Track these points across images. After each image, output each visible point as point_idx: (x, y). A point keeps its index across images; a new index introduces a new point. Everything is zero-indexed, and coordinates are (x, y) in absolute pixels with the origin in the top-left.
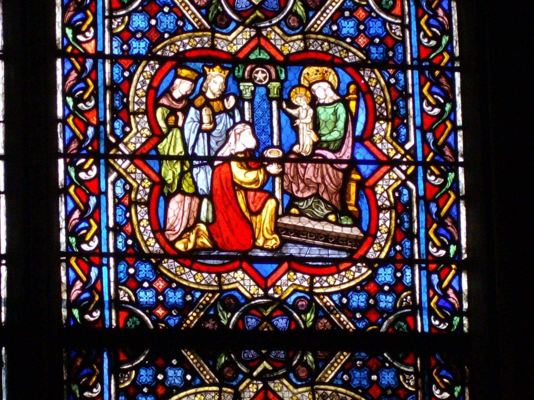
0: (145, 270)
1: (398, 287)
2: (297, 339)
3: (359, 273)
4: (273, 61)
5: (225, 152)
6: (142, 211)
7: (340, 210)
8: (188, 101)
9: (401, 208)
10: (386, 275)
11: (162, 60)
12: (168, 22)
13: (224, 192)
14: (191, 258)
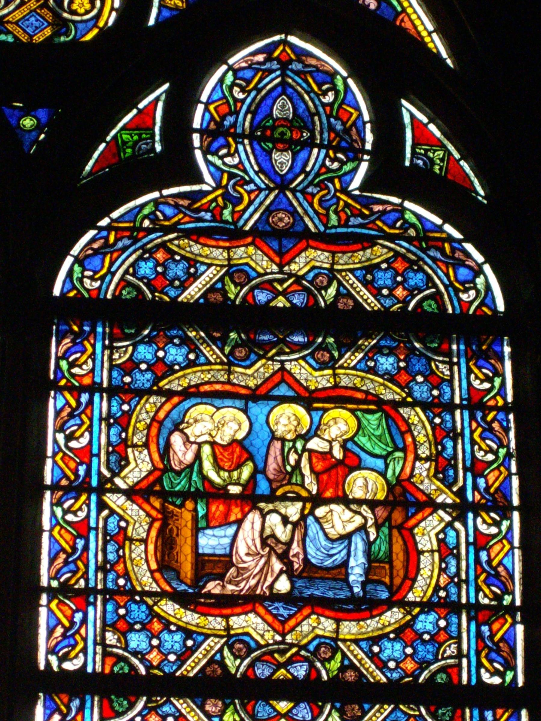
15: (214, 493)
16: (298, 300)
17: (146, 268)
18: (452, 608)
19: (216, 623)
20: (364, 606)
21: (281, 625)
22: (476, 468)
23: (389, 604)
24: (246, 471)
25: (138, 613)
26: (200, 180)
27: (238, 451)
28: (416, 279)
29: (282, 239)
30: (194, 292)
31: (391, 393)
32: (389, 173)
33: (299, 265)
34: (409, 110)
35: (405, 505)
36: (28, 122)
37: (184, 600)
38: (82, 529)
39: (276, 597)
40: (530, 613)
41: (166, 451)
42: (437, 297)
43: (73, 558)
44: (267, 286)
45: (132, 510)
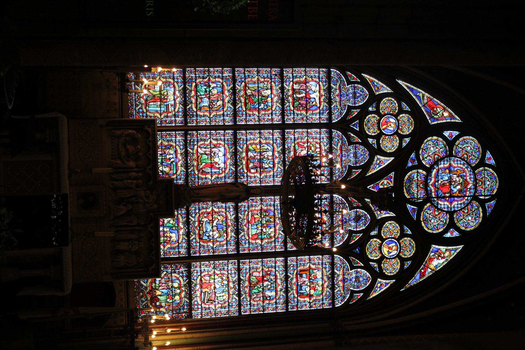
3: (200, 303)
6: (207, 273)
7: (208, 300)
8: (222, 279)
9: (209, 308)
12: (233, 275)
14: (201, 280)
15: (310, 275)
17: (338, 265)
18: (298, 302)
20: (297, 293)
22: (315, 304)
25: (295, 268)
27: (316, 277)
28: (339, 296)
29: (344, 280)
30: (336, 271)
31: (324, 294)
32: (353, 292)
33: (340, 283)
34: (362, 294)
38: (305, 261)
40: (297, 311)
41: (315, 269)
43: (301, 260)
44: (337, 279)
45: (308, 266)
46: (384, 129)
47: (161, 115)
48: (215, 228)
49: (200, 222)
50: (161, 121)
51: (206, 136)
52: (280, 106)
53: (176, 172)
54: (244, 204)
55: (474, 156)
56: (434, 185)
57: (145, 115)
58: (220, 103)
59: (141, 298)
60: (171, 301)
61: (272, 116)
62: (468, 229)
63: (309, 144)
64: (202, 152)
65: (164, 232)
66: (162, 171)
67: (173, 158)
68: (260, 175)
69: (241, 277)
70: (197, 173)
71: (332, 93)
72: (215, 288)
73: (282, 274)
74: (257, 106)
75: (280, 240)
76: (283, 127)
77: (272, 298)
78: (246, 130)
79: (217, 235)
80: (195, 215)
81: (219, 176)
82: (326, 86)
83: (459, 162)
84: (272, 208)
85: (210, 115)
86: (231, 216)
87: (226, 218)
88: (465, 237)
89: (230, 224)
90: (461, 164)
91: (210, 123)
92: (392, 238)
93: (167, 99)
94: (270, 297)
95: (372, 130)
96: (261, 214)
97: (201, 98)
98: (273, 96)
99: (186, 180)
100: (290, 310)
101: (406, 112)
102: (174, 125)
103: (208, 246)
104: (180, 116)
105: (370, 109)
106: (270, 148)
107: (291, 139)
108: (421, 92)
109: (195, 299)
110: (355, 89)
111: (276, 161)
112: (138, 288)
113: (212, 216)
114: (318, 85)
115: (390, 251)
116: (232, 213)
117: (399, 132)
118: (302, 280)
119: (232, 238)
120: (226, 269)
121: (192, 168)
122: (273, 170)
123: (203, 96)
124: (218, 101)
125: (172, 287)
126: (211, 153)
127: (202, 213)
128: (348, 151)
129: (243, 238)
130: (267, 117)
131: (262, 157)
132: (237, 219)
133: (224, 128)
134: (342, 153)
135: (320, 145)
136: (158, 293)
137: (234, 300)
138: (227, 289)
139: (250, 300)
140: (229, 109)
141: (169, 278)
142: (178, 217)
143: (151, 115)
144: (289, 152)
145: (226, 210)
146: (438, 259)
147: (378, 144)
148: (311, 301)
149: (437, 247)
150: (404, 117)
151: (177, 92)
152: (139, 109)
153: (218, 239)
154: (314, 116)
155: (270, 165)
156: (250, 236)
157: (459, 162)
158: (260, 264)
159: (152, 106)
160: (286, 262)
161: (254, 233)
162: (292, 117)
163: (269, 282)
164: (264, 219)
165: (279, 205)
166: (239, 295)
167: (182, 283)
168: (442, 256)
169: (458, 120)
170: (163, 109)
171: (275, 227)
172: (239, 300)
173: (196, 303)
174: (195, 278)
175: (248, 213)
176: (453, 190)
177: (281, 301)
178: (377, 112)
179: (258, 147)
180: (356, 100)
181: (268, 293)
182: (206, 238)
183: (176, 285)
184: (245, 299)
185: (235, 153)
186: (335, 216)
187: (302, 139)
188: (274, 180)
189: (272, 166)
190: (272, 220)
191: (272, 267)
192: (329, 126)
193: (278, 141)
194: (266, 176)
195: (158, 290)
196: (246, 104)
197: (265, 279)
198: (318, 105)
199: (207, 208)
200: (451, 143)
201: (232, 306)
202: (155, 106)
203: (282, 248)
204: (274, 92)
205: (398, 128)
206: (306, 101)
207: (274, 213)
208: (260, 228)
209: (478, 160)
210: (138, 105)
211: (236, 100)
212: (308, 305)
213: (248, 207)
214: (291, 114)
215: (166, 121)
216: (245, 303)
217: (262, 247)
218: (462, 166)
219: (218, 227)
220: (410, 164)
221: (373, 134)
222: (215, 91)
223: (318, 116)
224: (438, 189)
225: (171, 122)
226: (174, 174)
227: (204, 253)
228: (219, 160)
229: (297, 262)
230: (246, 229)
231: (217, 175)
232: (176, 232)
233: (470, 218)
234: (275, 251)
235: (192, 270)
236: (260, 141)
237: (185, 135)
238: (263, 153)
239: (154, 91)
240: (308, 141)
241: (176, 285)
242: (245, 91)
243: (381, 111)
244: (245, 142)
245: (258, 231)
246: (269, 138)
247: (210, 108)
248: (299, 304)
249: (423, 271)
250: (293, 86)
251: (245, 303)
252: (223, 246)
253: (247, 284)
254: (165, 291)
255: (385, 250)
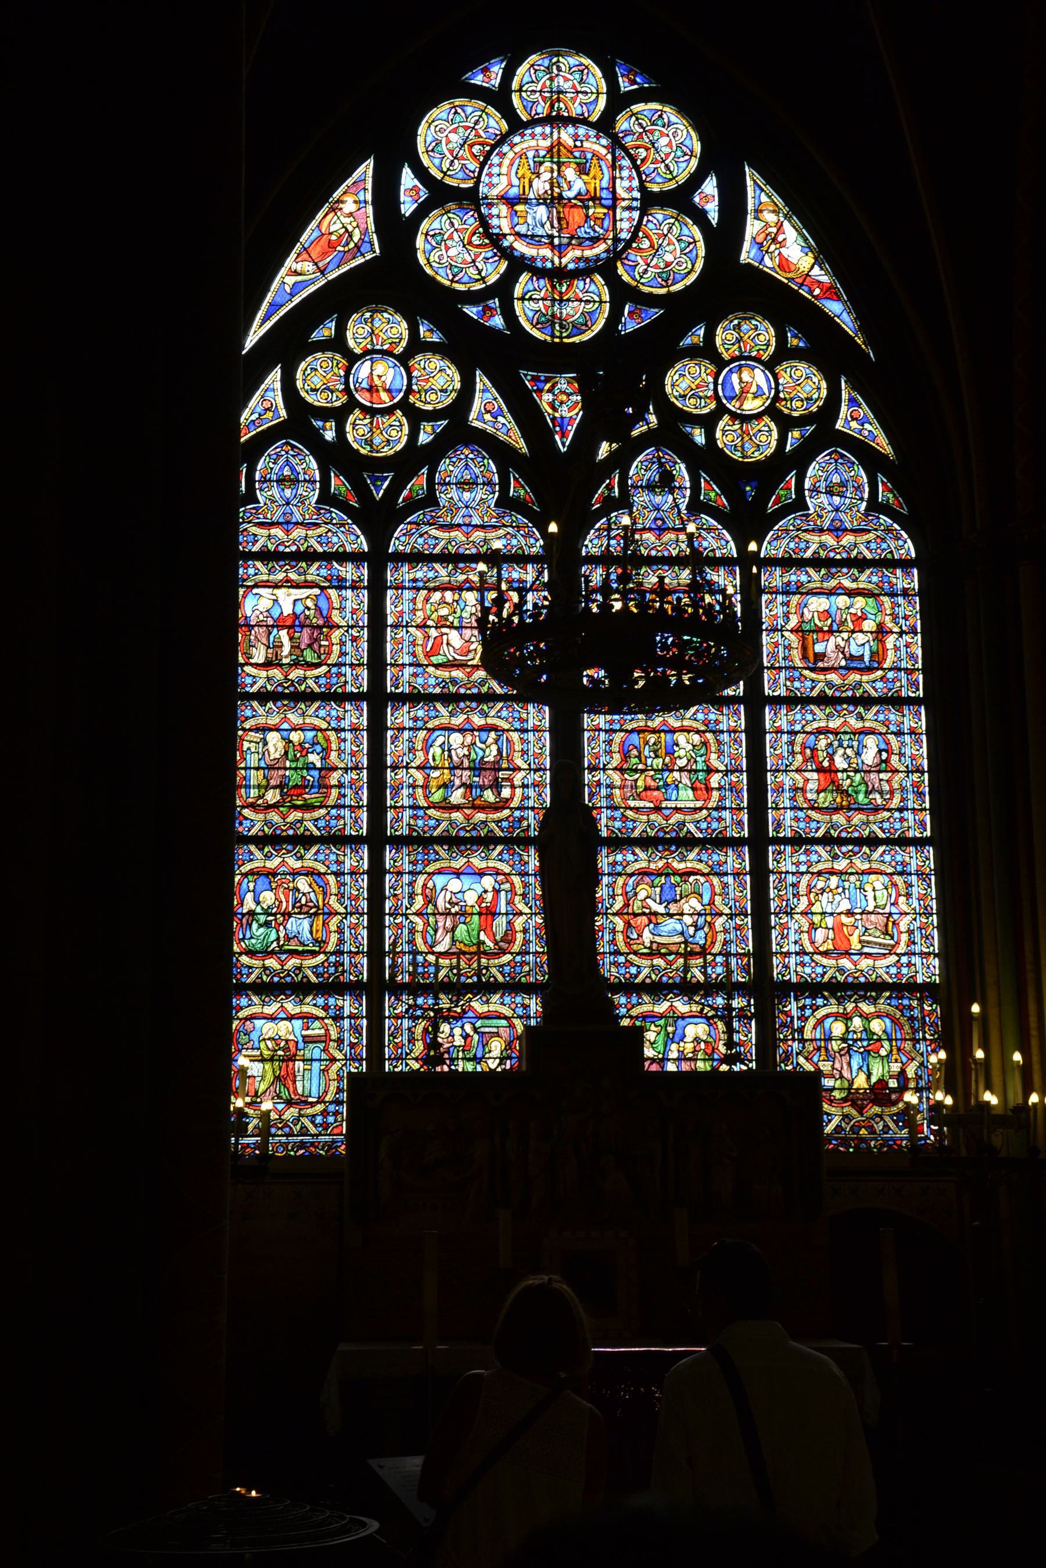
0: (807, 959)
1: (909, 965)
2: (869, 986)
3: (893, 959)
4: (857, 873)
5: (838, 911)
6: (806, 936)
7: (886, 933)
8: (823, 890)
9: (910, 932)
10: (904, 960)
11: (813, 873)
13: (838, 928)
14: (826, 954)
15: (819, 630)
16: (844, 555)
17: (792, 545)
18: (900, 669)
19: (822, 677)
20: (870, 670)
21: (843, 677)
22: (906, 618)
23: (877, 669)
24: (829, 621)
25: (797, 674)
26: (808, 509)
27: (827, 612)
28: (884, 546)
29: (838, 530)
35: (882, 632)
36: (748, 489)
37: (812, 670)
38: (776, 644)
39: (841, 668)
40: (924, 670)
42: (891, 552)
43: (773, 655)
44: (834, 550)
46: (392, 398)
47: (333, 1060)
48: (673, 908)
49: (654, 952)
50: (352, 1059)
51: (400, 926)
52: (316, 705)
53: (506, 1018)
54: (604, 821)
55: (476, 123)
56: (560, 250)
57: (332, 1108)
58: (303, 884)
59: (874, 1132)
60: (886, 1044)
61: (344, 730)
62: (698, 147)
63: (430, 623)
64: (448, 939)
65: (681, 1058)
66: (502, 1060)
67: (462, 1027)
68: (519, 769)
69: (820, 834)
70: (507, 958)
71: (281, 548)
72: (850, 913)
73: (812, 713)
74: (316, 773)
75: (712, 717)
76: (378, 699)
77: (883, 746)
78: (384, 809)
79: (694, 902)
80: (632, 964)
81: (520, 891)
82: (259, 564)
83: (495, 170)
84: (618, 737)
85: (337, 913)
86: (640, 859)
87: (644, 873)
88: (720, 159)
89: (661, 864)
90: (500, 165)
91: (362, 914)
92: (716, 384)
93: (287, 1041)
94: (880, 751)
95: (394, 433)
96: (636, 771)
97: (288, 938)
98: (285, 726)
99: (529, 989)
100: (921, 693)
101: (341, 329)
102: (365, 1021)
103: (726, 931)
104: (340, 1003)
105: (329, 435)
106: (440, 740)
107: (415, 675)
108: (284, 280)
109: (881, 972)
110: (270, 480)
111: (478, 721)
112: (845, 1142)
113: (636, 915)
114: (255, 591)
115: (754, 389)
116: (630, 857)
117: (398, 350)
118: (833, 655)
119: (704, 857)
120: (794, 879)
121: (494, 970)
122: (504, 730)
123: (282, 935)
124: (298, 890)
125: (844, 1040)
126: (449, 914)
127: (628, 944)
128: (453, 508)
129: (704, 825)
130: (348, 746)
131: (466, 764)
132: (645, 842)
133: (377, 872)
134: (459, 525)
135: (435, 589)
136: (861, 1082)
137: (887, 858)
138: (852, 878)
139: (889, 810)
140: (321, 857)
141: (819, 1049)
142: (637, 1018)
143: (333, 1088)
144: (454, 681)
145: (620, 874)
146: (782, 244)
147: (433, 416)
148: (896, 629)
149: (746, 246)
150: (356, 334)
151: (269, 1010)
152: (315, 1126)
153: (706, 900)
154: (349, 604)
155: (490, 740)
156: (699, 804)
157: (495, 170)
158: (781, 777)
159: (307, 1085)
160: (777, 701)
161: (690, 792)
162: (349, 670)
163: (834, 753)
164: (649, 761)
165: (609, 717)
166: (873, 842)
167: (833, 1009)
168: (774, 230)
169: (366, 170)
170: (317, 1053)
171: (673, 731)
172: (887, 842)
173: (893, 970)
174: (819, 970)
175: (631, 809)
176: (579, 194)
177: (892, 717)
178: (339, 415)
179: (436, 774)
180: (301, 477)
181: (869, 757)
182: (701, 934)
183: (838, 1029)
184: (886, 825)
185: (453, 842)
186: (644, 552)
187: (414, 643)
188: (536, 729)
189: (493, 735)
190: (652, 738)
191: (792, 743)
192: (378, 559)
193: (421, 713)
194: (524, 752)
195: (851, 1083)
196: (308, 807)
197: (826, 764)
198: (317, 591)
199: (614, 931)
200: (439, 195)
201: (904, 864)
202: (307, 1075)
203: (737, 713)
204: (273, 720)
205: (388, 353)
206: (302, 626)
207: (632, 731)
208: (676, 774)
209: (490, 109)
210: (303, 1127)
211: (295, 835)
212: (907, 638)
213: (614, 808)
214: (339, 675)
215: (352, 1046)
216: (897, 826)
217: (733, 772)
218: (506, 162)
219: (669, 897)
220: (498, 321)
221: (406, 429)
222: (268, 898)
223: (349, 593)
224: (572, 237)
225: (356, 1030)
226: (512, 1026)
227: (745, 940)
228: (471, 892)
229: (780, 668)
230: (678, 817)
231: (517, 899)
232: (680, 1023)
233: (664, 141)
234: (746, 731)
235: (794, 980)
236: (418, 768)
237: (397, 989)
238: (455, 758)
239: (263, 1078)
240: (423, 626)
241: (838, 1029)
242: (269, 807)
243: (338, 404)
244: (421, 813)
245: (686, 780)
246: (410, 740)
247: (316, 914)
248: (903, 665)
249: (817, 292)
250: (256, 666)
251: (897, 826)
252: (725, 885)
253: (839, 818)
254: (856, 1061)
255: (752, 406)
